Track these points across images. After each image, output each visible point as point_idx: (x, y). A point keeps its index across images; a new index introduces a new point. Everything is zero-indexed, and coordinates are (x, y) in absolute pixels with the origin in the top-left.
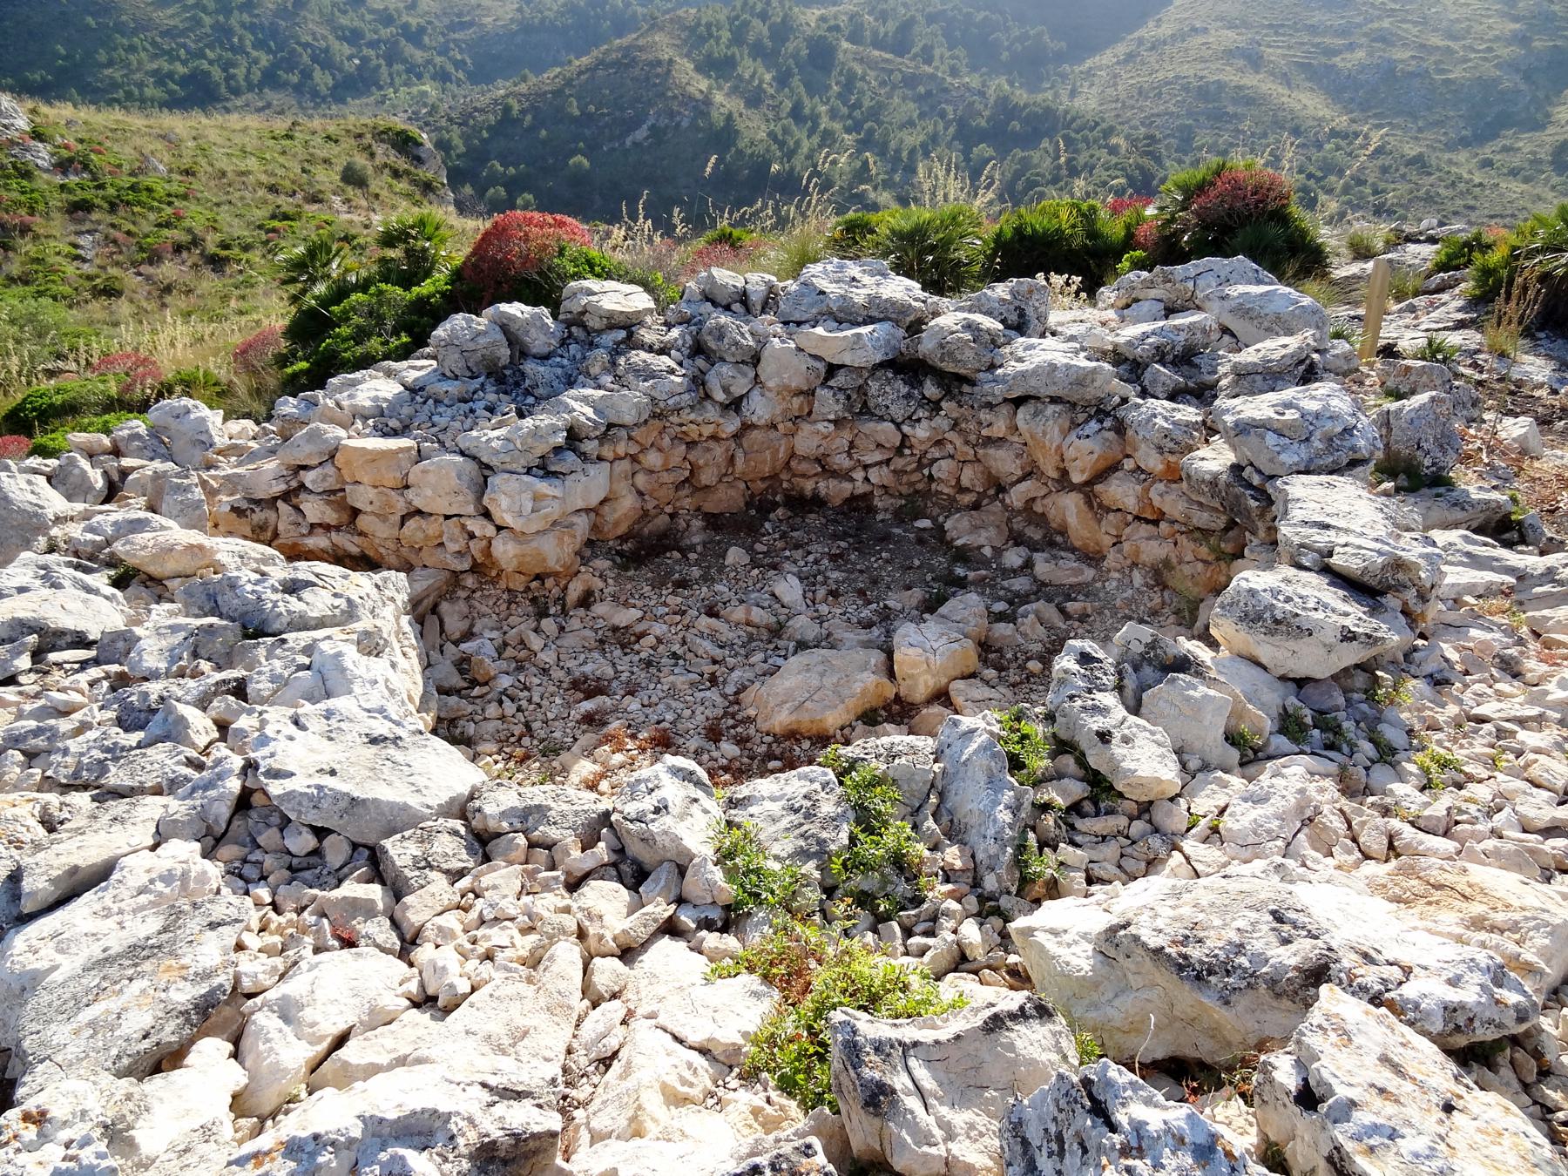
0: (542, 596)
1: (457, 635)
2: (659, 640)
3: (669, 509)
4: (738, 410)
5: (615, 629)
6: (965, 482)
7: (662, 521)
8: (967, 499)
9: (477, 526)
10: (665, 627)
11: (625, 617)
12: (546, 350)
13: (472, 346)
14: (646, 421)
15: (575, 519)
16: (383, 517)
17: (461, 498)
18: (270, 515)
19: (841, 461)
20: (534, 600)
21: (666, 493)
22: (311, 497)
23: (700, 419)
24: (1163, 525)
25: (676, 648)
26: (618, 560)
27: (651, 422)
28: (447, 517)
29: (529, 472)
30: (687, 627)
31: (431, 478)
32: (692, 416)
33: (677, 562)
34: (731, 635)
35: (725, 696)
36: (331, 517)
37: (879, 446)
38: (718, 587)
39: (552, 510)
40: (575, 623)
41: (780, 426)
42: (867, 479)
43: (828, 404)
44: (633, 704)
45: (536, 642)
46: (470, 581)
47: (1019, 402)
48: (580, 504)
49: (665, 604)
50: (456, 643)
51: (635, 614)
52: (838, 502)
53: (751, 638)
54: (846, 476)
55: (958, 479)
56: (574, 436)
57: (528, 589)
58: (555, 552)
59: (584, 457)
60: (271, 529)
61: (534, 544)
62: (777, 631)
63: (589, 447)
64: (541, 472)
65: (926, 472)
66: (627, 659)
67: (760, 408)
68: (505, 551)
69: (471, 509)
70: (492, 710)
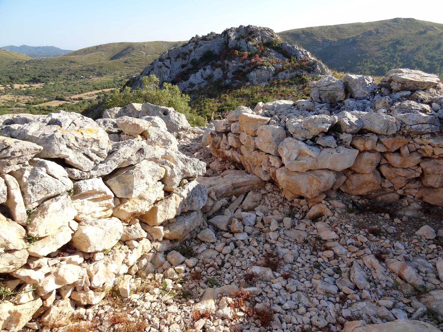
0: (295, 208)
1: (246, 208)
2: (336, 256)
3: (400, 192)
5: (318, 238)
7: (392, 197)
9: (274, 162)
10: (344, 250)
11: (328, 234)
12: (362, 96)
13: (324, 88)
14: (394, 135)
15: (325, 173)
16: (248, 148)
17: (271, 145)
18: (219, 138)
20: (292, 207)
21: (399, 182)
23: (436, 143)
25: (343, 266)
26: (350, 206)
27: (398, 137)
29: (305, 141)
30: (359, 258)
32: (431, 141)
33: (385, 220)
34: (381, 276)
35: (339, 314)
36: (235, 145)
38: (398, 244)
39: (308, 163)
40: (302, 226)
44: (278, 284)
45: (274, 226)
46: (269, 187)
48: (328, 166)
49: (356, 239)
50: (243, 211)
51: (334, 235)
53: (396, 287)
56: (336, 129)
57: (292, 201)
58: (307, 186)
59: (340, 143)
60: (218, 144)
61: (294, 178)
62: (419, 292)
63: (343, 137)
64: (311, 143)
66: (308, 257)
68: (281, 176)
69: (272, 152)
70: (219, 246)
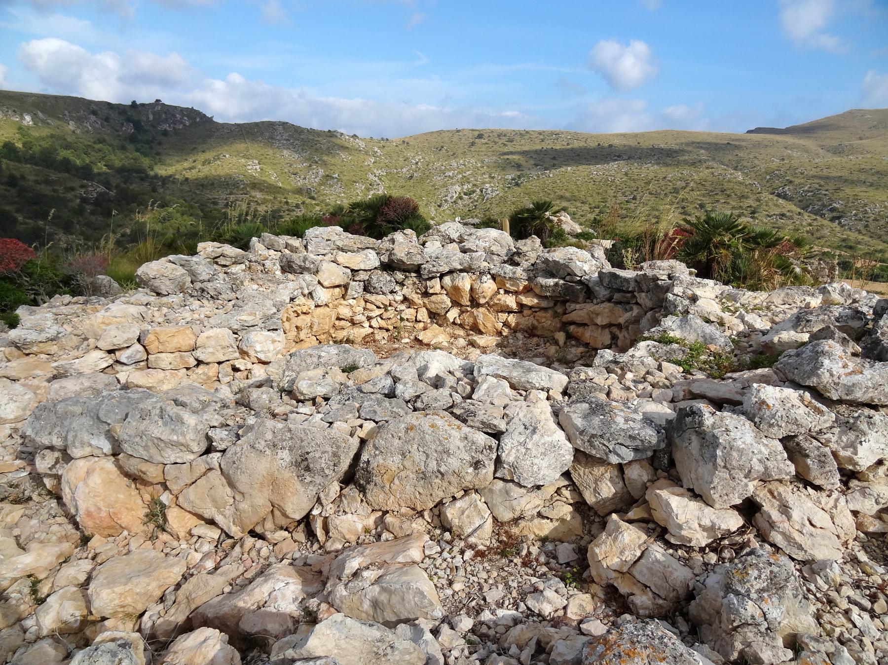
4: (312, 298)
6: (419, 318)
8: (421, 325)
19: (359, 318)
22: (125, 368)
24: (526, 312)
28: (219, 363)
31: (213, 343)
37: (378, 307)
41: (330, 305)
42: (371, 326)
43: (356, 288)
47: (442, 277)
52: (360, 339)
54: (360, 325)
67: (323, 296)
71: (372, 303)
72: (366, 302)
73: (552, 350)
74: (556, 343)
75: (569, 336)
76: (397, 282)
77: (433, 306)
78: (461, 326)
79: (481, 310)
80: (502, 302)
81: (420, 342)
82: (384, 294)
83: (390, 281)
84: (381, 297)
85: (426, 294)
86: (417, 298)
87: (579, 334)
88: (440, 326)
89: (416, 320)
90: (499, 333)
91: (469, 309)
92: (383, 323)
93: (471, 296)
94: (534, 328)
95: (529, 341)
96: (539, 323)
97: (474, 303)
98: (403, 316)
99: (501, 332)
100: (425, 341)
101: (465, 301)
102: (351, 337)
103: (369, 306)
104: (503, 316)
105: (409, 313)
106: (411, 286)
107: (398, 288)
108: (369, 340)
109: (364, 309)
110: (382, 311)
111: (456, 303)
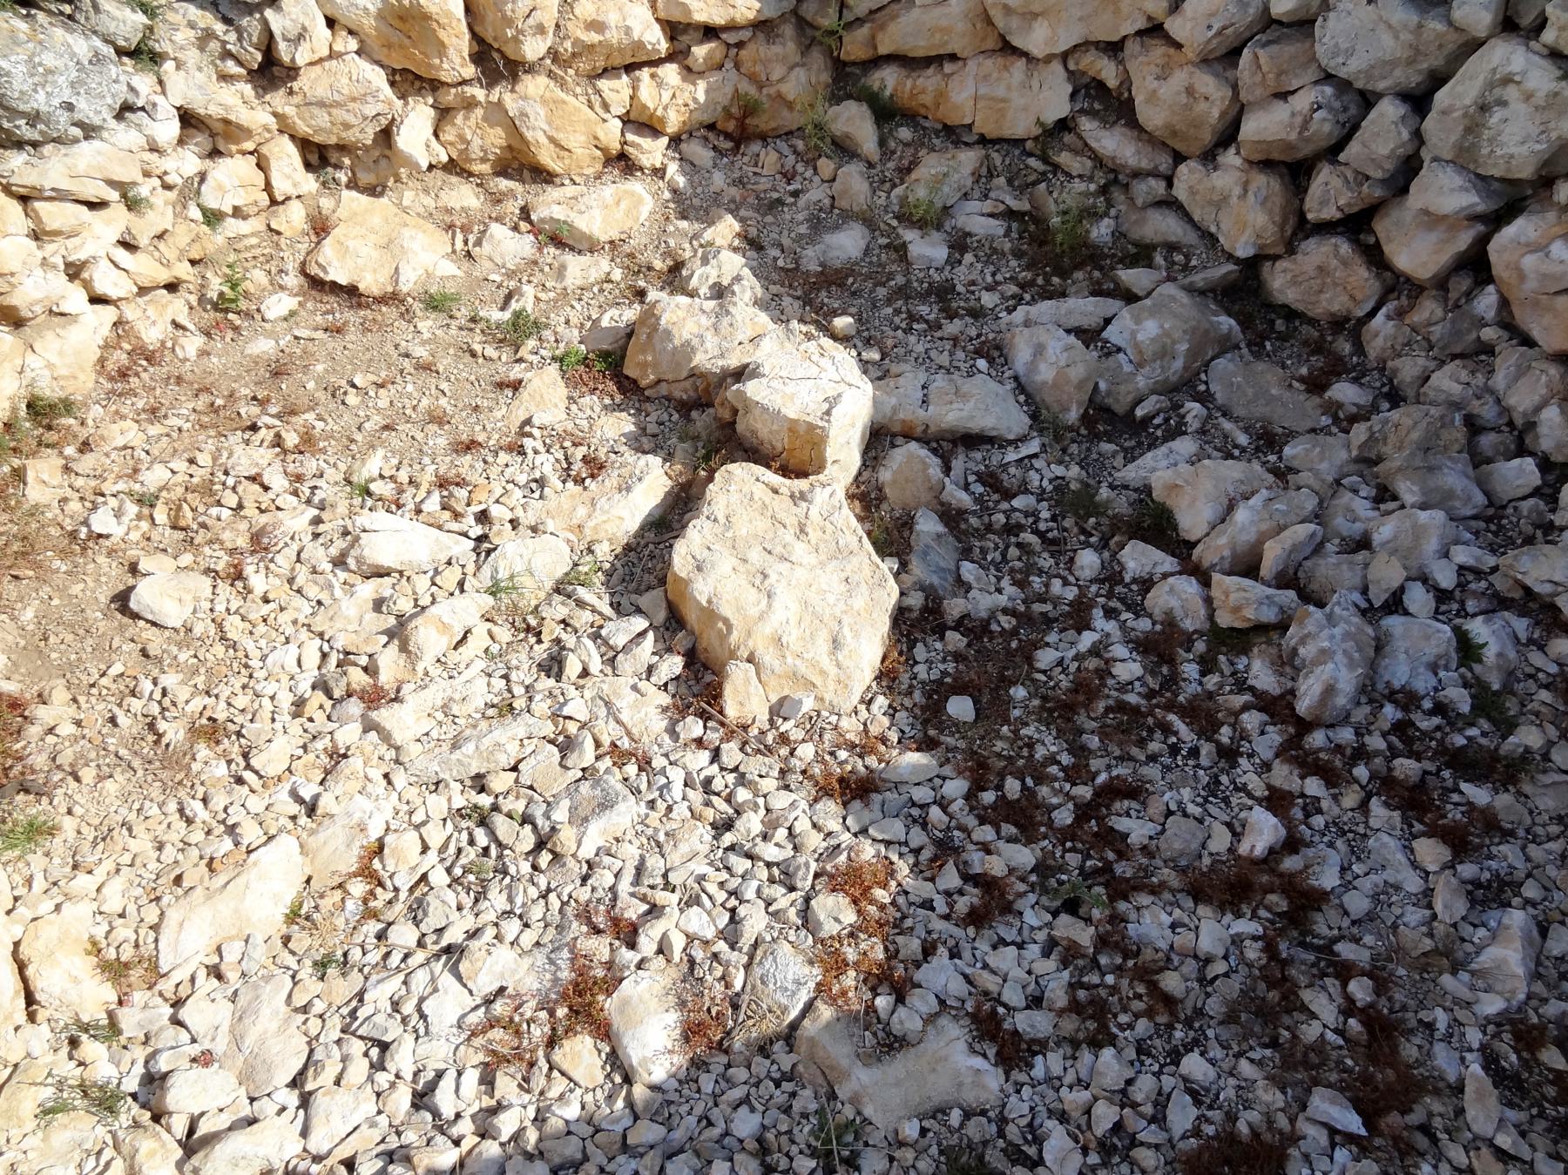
42: (96, 300)
55: (268, 188)
65: (194, 213)
71: (60, 196)
72: (24, 199)
73: (854, 182)
74: (844, 150)
75: (886, 113)
76: (121, 52)
77: (322, 119)
78: (454, 167)
79: (534, 85)
80: (613, 36)
81: (351, 292)
82: (90, 131)
83: (97, 59)
84: (87, 154)
85: (271, 71)
86: (234, 101)
87: (927, 99)
88: (374, 191)
89: (274, 202)
90: (622, 162)
91: (479, 93)
92: (144, 266)
93: (475, 35)
94: (749, 109)
95: (743, 163)
96: (760, 88)
97: (496, 62)
98: (212, 202)
99: (622, 156)
100: (371, 283)
101: (456, 62)
102: (49, 391)
103: (53, 214)
104: (617, 90)
105: (232, 179)
106: (192, 56)
107: (144, 83)
108: (127, 363)
109: (38, 235)
110: (118, 212)
111: (409, 81)
